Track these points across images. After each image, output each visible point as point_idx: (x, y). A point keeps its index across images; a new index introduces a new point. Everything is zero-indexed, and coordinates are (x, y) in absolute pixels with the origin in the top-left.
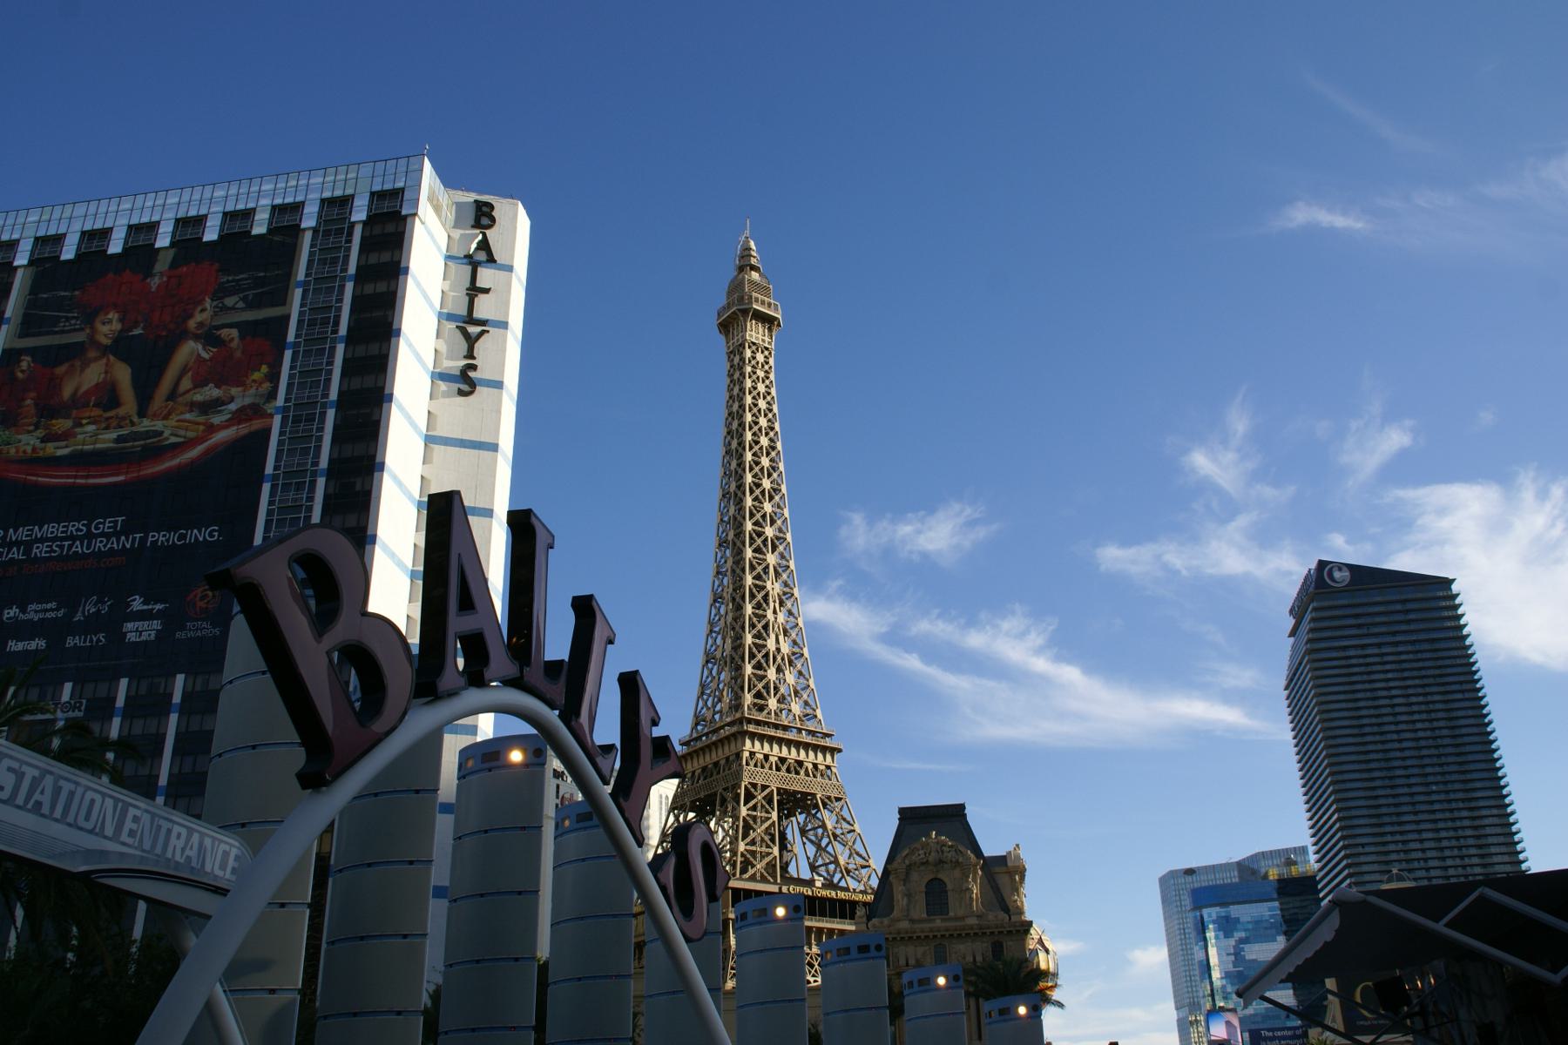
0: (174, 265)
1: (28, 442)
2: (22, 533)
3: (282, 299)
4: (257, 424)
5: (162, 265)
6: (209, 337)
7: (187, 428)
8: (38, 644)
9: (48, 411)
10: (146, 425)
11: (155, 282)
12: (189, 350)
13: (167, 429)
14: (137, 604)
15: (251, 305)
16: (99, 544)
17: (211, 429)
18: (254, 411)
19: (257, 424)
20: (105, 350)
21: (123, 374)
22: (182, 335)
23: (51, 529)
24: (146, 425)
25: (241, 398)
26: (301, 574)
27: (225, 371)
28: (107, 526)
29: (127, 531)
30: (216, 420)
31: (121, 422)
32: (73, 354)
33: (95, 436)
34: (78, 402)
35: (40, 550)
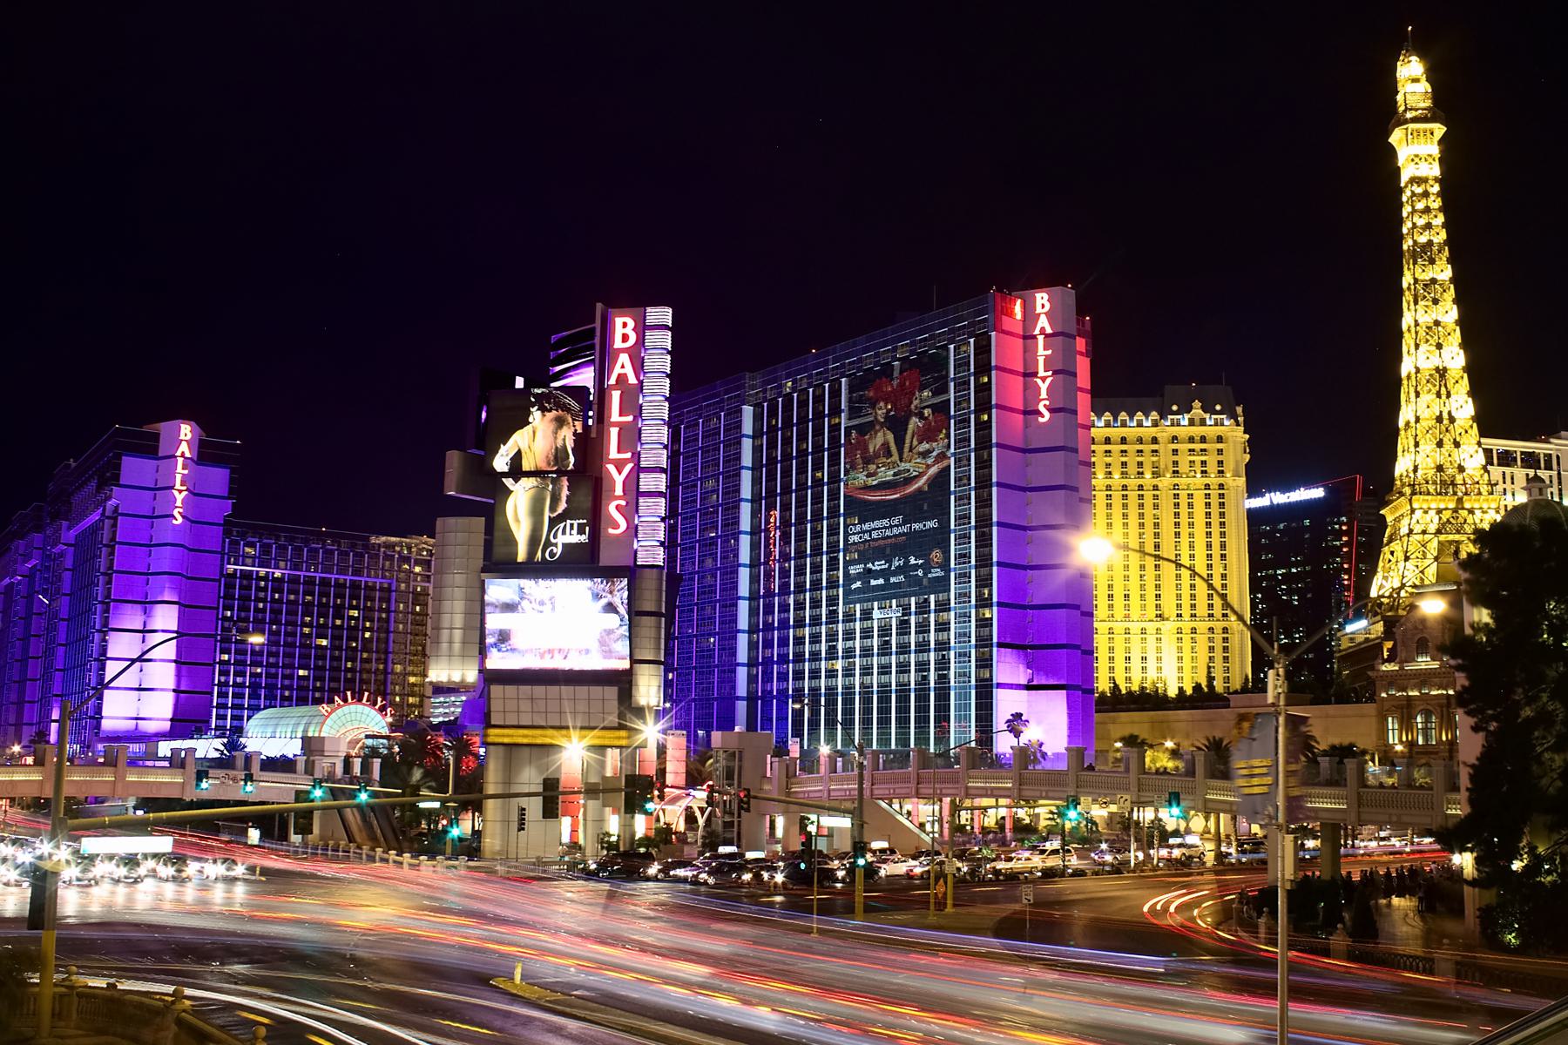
0: (901, 372)
1: (861, 478)
2: (866, 527)
3: (946, 391)
4: (945, 463)
5: (896, 374)
6: (921, 416)
7: (920, 469)
8: (881, 581)
9: (867, 461)
10: (903, 466)
11: (895, 383)
12: (914, 422)
13: (911, 466)
14: (913, 561)
15: (935, 393)
16: (895, 531)
17: (928, 467)
18: (942, 456)
19: (945, 463)
20: (882, 425)
21: (890, 437)
22: (910, 414)
23: (877, 524)
24: (903, 466)
25: (937, 447)
26: (1108, 416)
27: (928, 434)
28: (896, 520)
29: (904, 523)
30: (930, 461)
31: (894, 464)
32: (871, 425)
33: (886, 475)
34: (876, 455)
35: (875, 534)
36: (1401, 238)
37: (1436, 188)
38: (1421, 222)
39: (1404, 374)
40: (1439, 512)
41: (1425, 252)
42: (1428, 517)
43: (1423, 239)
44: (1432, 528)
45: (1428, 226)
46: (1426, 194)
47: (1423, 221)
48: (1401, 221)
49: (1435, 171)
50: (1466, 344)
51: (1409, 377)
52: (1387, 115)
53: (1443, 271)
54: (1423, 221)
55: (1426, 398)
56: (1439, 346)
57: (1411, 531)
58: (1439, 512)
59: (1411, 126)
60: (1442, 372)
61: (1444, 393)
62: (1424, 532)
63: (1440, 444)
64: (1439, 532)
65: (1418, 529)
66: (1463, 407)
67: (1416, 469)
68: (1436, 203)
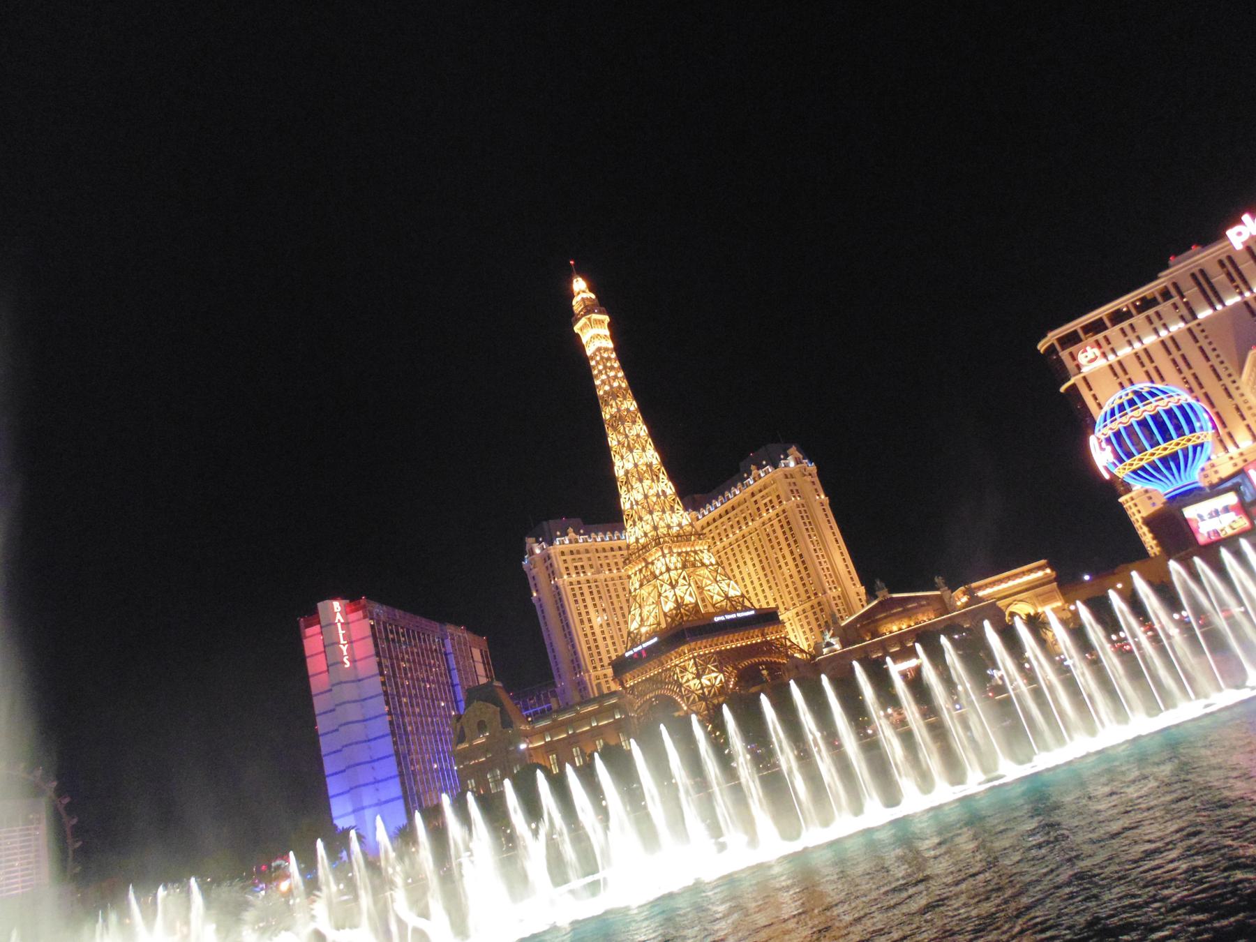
36: (593, 388)
37: (613, 355)
38: (612, 374)
39: (619, 472)
40: (679, 554)
41: (613, 394)
42: (674, 559)
43: (616, 384)
44: (679, 565)
45: (616, 377)
46: (609, 359)
47: (609, 377)
48: (591, 378)
49: (610, 345)
50: (658, 448)
51: (627, 472)
52: (569, 317)
53: (631, 405)
54: (609, 377)
55: (647, 483)
56: (644, 450)
57: (668, 570)
58: (679, 554)
59: (594, 316)
60: (650, 466)
61: (655, 477)
62: (676, 569)
63: (664, 512)
64: (684, 567)
65: (672, 567)
66: (668, 487)
67: (655, 528)
68: (617, 365)
